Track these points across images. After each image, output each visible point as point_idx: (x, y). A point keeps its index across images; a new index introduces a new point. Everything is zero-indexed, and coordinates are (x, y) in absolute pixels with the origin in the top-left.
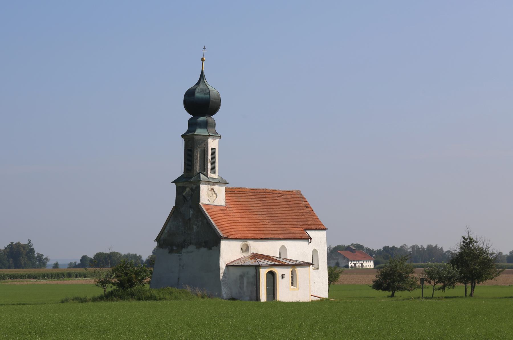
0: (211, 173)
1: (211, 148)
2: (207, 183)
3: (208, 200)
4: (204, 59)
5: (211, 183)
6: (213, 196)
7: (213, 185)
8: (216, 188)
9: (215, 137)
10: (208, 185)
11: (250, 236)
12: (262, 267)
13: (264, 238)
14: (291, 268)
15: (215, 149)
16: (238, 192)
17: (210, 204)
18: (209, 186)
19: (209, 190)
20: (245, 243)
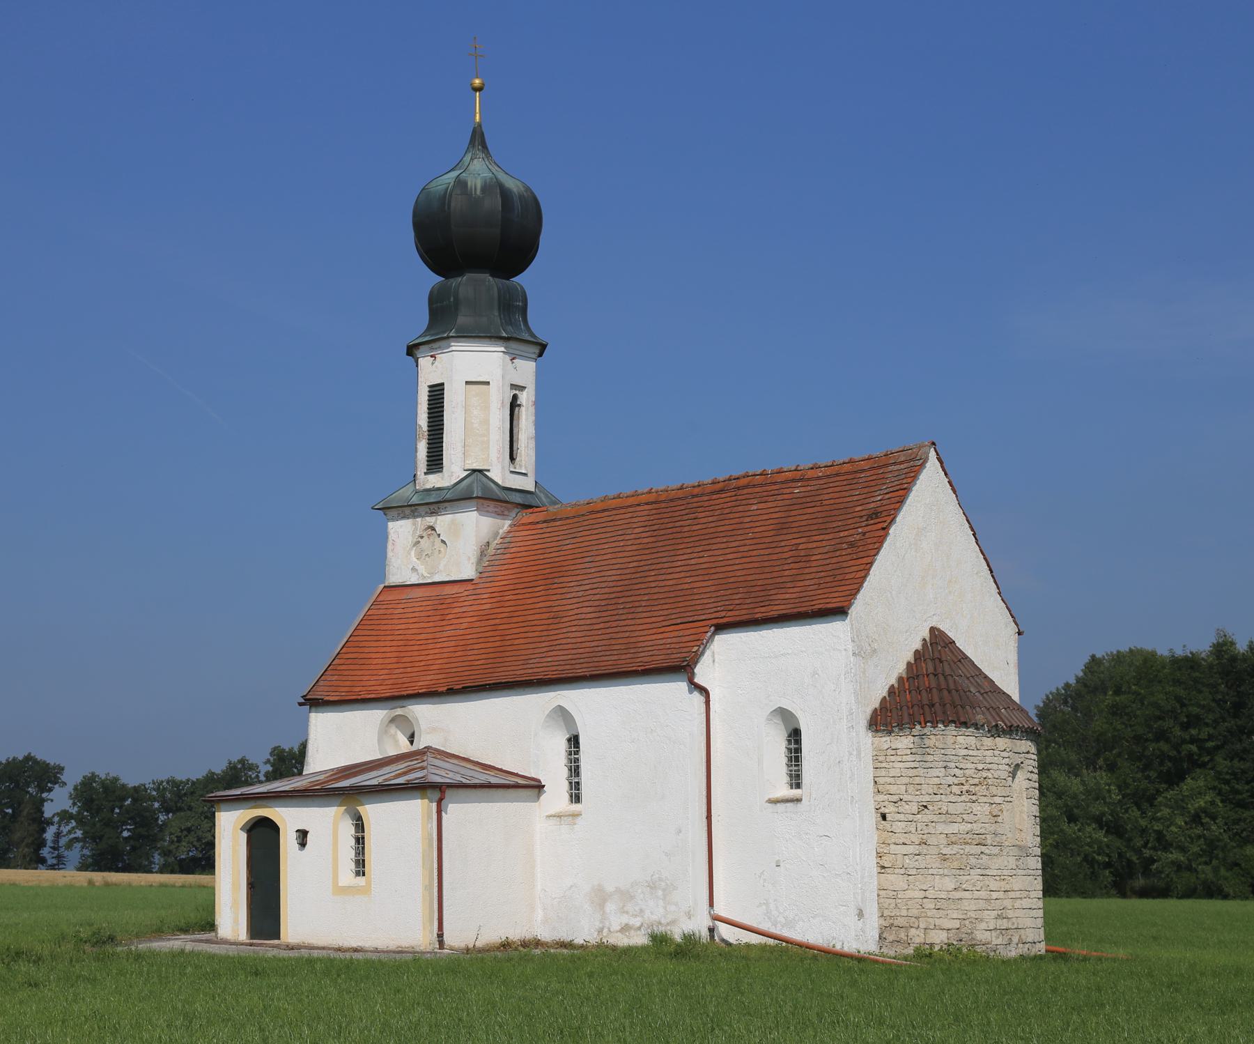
0: (425, 474)
1: (430, 387)
2: (407, 511)
3: (414, 569)
4: (477, 82)
5: (422, 509)
6: (436, 552)
7: (433, 513)
8: (443, 522)
9: (435, 345)
10: (415, 517)
11: (421, 685)
12: (222, 806)
13: (463, 688)
14: (340, 805)
15: (443, 384)
16: (598, 512)
17: (421, 582)
18: (419, 520)
19: (418, 533)
20: (399, 712)
